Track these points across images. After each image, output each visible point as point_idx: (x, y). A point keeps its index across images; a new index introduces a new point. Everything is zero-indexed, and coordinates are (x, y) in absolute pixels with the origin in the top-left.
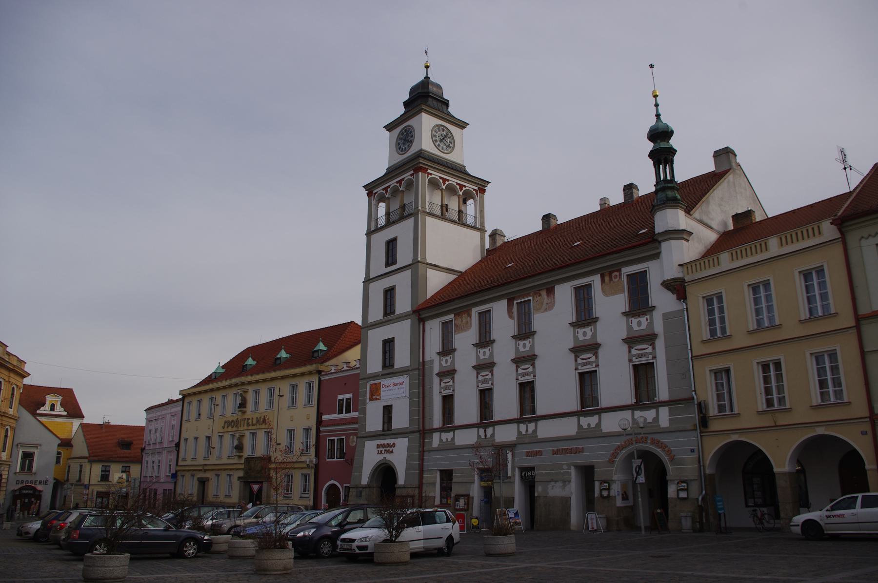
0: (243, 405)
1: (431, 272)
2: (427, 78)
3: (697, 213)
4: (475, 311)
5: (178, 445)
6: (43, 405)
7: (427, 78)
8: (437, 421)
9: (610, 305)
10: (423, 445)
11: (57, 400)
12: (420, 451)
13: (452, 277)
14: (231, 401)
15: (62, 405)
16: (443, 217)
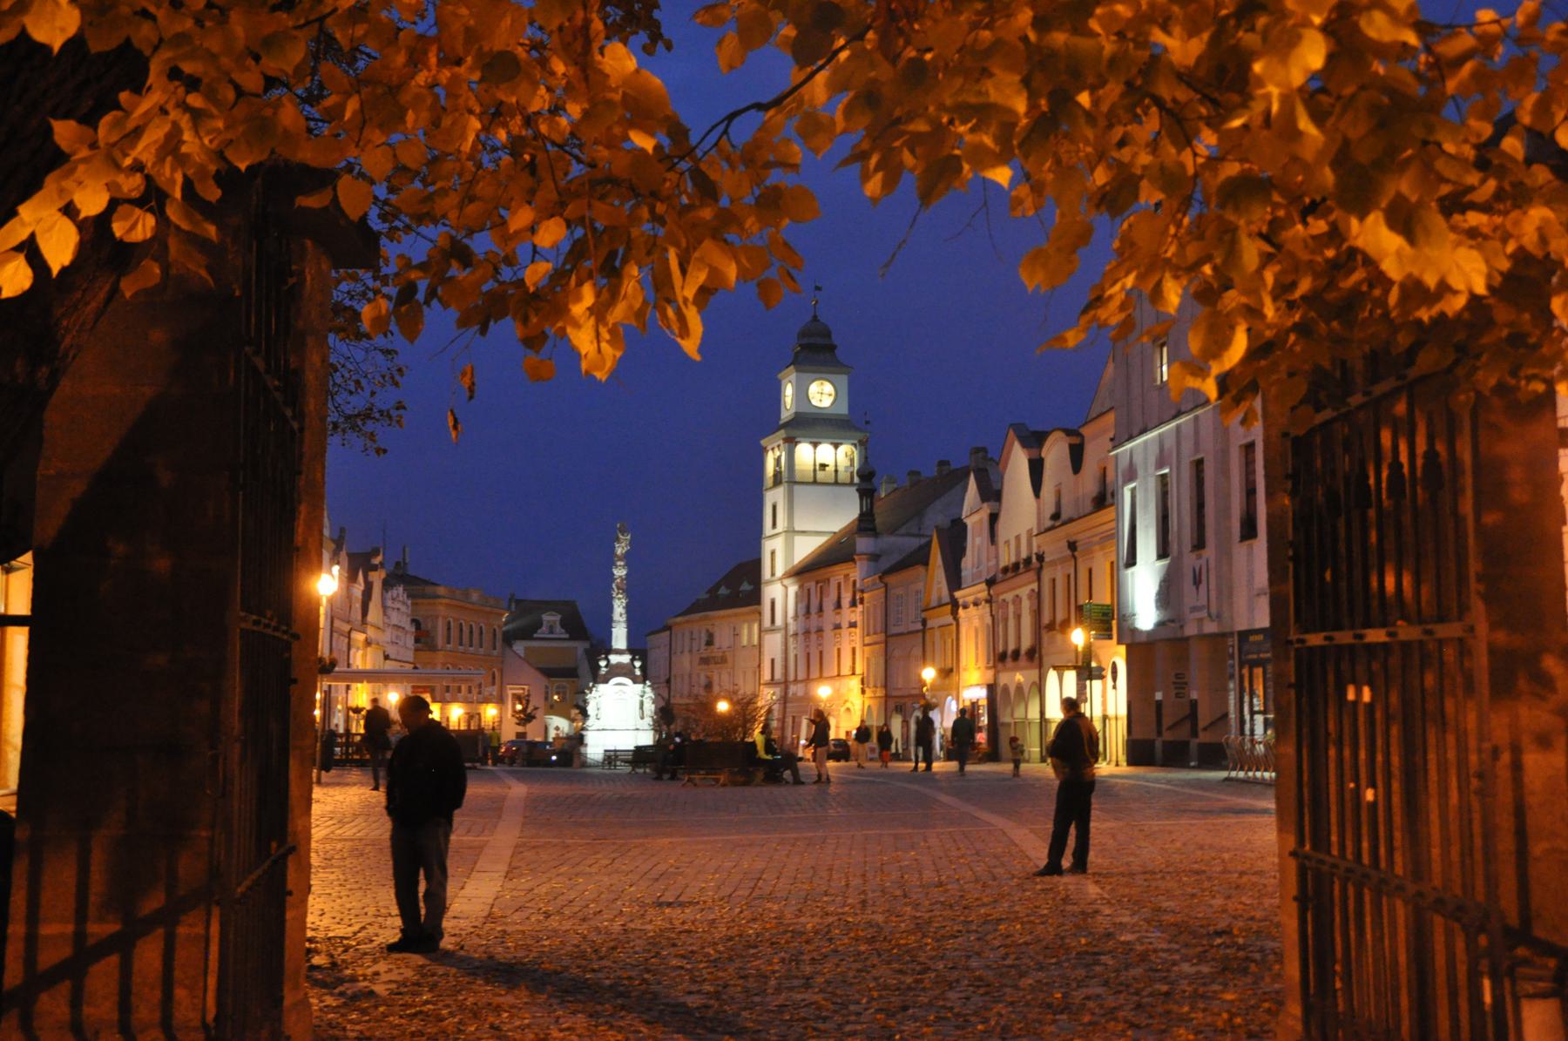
0: (710, 643)
1: (798, 539)
2: (815, 317)
3: (903, 531)
4: (807, 585)
5: (668, 681)
6: (540, 625)
7: (815, 317)
8: (791, 678)
9: (846, 599)
10: (786, 693)
11: (558, 617)
12: (784, 699)
13: (820, 541)
14: (704, 638)
15: (563, 624)
16: (815, 482)
